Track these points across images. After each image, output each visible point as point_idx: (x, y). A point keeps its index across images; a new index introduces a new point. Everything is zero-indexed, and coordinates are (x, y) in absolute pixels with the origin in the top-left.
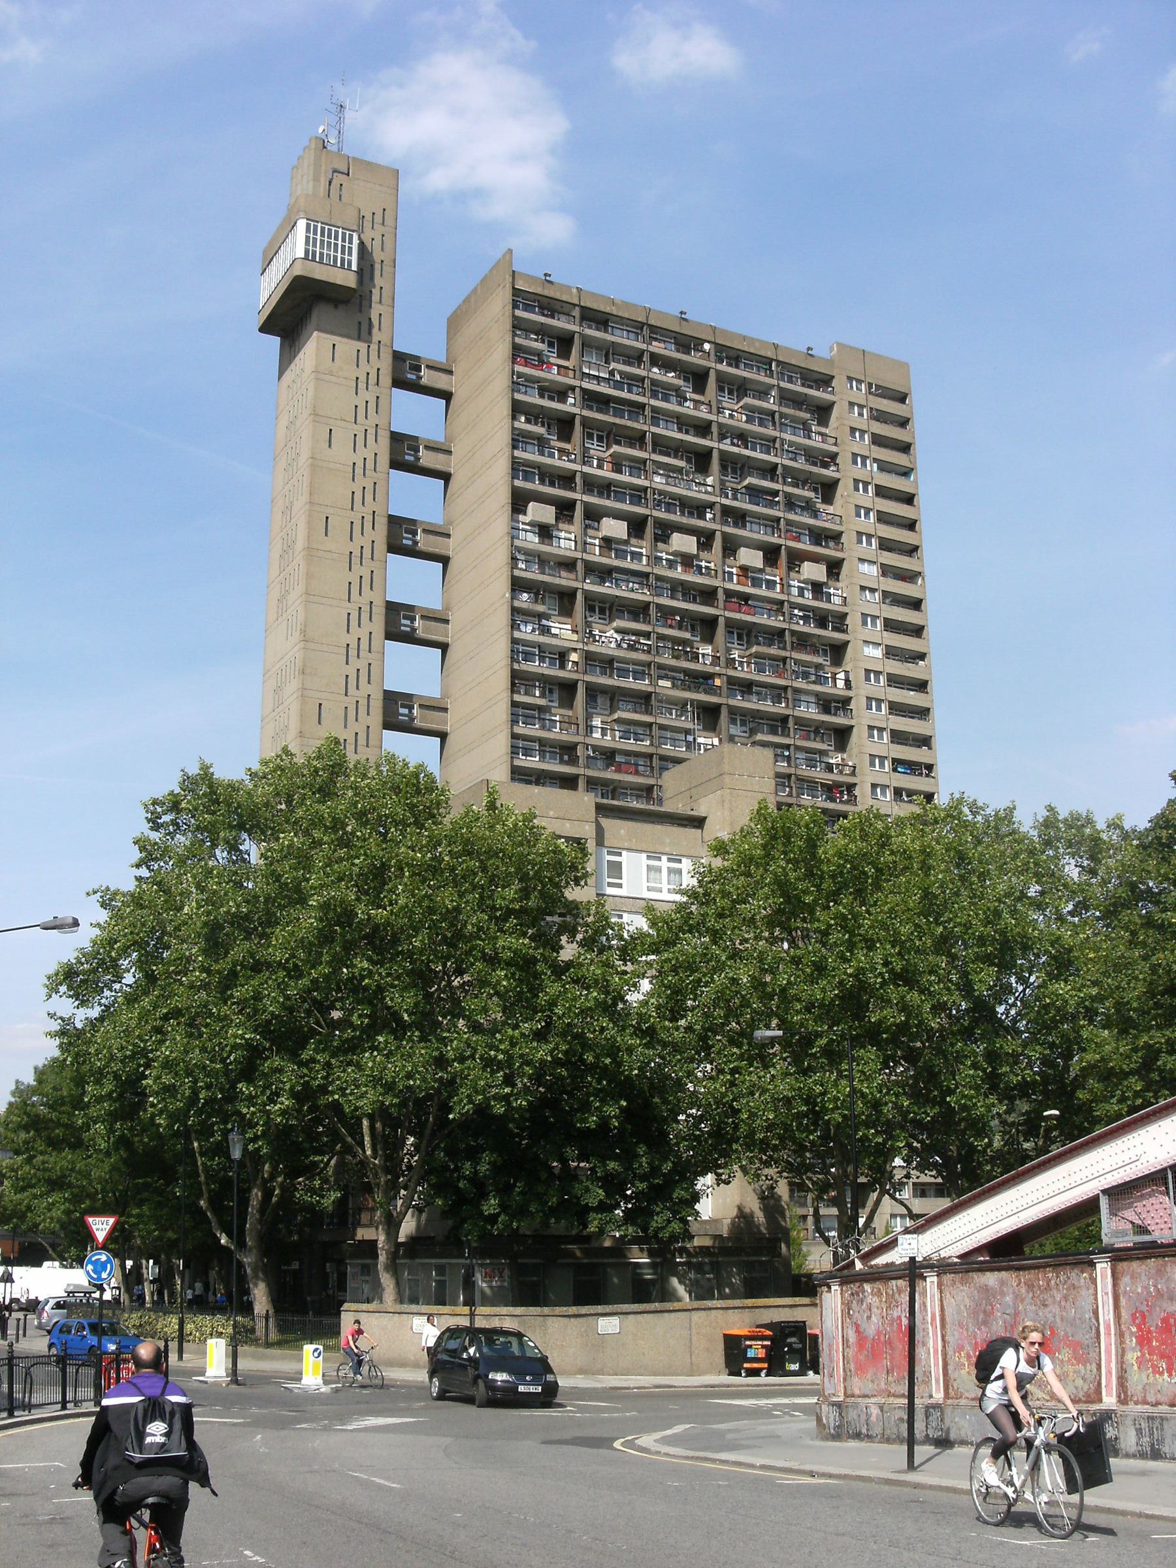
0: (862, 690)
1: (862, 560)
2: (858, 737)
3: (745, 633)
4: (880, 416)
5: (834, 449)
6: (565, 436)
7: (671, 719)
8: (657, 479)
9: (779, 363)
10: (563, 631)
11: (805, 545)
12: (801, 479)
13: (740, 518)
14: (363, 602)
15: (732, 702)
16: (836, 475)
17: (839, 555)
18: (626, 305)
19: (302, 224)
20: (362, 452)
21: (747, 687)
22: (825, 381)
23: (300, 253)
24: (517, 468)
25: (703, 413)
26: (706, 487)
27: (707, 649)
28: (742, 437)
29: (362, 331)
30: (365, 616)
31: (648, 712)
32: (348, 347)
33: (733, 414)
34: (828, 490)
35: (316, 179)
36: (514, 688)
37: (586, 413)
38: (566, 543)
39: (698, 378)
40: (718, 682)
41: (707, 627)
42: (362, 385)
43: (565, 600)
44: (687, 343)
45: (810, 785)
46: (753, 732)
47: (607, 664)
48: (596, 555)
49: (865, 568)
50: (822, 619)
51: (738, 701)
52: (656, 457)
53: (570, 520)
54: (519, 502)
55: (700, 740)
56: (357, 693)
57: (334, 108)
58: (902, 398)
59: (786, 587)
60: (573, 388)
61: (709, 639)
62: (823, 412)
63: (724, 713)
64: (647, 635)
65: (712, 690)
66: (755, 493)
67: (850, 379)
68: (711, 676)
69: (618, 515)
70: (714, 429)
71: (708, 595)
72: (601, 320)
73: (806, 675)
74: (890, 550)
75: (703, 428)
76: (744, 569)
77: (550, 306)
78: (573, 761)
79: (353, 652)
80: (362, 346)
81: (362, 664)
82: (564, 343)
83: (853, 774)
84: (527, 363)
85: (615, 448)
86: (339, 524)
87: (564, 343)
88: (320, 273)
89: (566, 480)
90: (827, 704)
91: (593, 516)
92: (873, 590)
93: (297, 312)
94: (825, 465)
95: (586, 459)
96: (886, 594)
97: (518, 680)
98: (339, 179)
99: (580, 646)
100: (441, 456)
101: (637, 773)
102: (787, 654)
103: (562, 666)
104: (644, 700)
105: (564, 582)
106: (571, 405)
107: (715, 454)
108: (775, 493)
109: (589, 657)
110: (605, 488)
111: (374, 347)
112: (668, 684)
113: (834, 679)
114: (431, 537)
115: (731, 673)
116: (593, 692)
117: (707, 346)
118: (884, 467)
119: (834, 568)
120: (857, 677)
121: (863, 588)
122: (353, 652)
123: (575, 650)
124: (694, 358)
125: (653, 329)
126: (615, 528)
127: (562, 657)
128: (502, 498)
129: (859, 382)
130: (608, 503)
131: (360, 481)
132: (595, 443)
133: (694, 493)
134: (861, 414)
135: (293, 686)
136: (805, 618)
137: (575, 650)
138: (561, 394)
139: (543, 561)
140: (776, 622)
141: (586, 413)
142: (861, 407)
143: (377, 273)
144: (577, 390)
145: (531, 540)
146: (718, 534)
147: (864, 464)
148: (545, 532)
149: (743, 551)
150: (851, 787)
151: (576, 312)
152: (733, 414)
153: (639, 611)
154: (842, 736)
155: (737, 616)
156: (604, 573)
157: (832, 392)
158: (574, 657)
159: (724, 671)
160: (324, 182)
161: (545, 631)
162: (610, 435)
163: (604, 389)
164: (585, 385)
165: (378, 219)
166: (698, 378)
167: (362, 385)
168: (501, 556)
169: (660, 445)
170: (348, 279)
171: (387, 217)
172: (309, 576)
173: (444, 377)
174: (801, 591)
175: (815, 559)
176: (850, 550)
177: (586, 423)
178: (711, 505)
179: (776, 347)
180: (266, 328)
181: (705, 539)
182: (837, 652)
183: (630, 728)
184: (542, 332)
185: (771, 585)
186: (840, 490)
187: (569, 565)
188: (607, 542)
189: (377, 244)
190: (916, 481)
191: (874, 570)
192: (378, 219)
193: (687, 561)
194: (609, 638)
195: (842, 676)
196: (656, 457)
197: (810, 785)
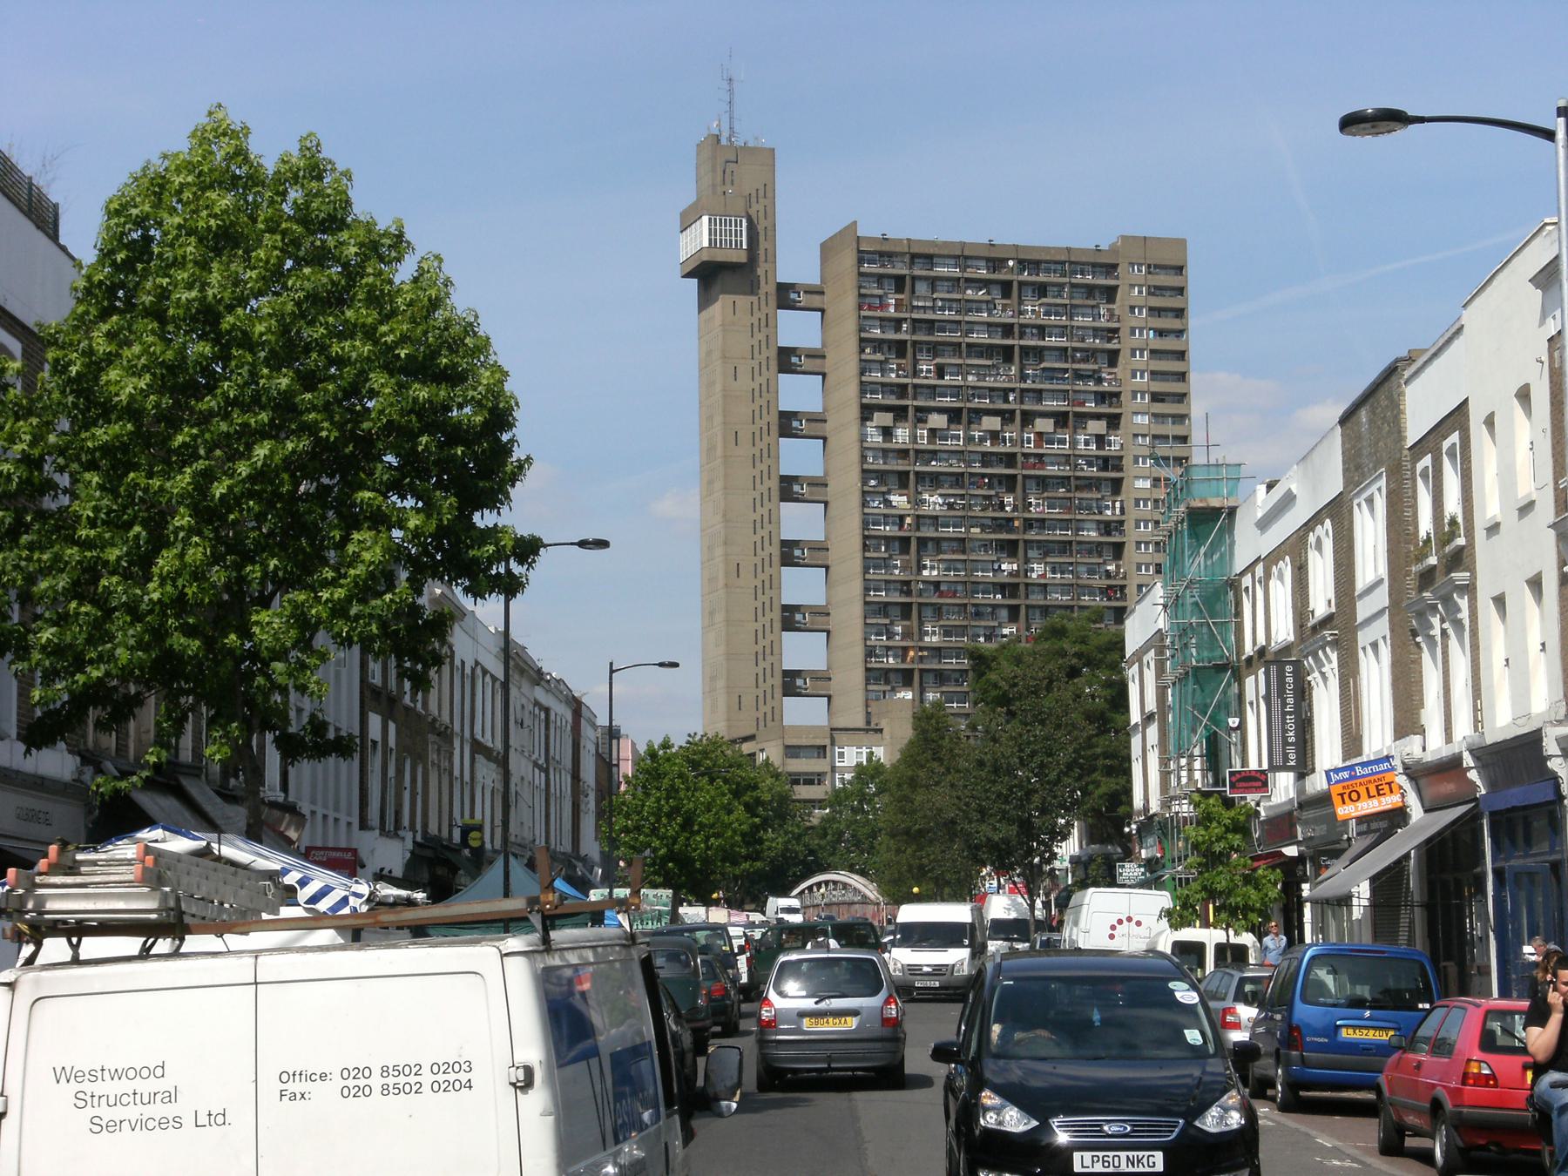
0: (1132, 515)
1: (1137, 413)
2: (1129, 551)
3: (1043, 483)
4: (1156, 290)
5: (1115, 325)
6: (901, 353)
7: (982, 556)
8: (970, 378)
9: (1071, 263)
10: (899, 500)
11: (1091, 406)
12: (1090, 354)
13: (1039, 395)
15: (1027, 537)
16: (1117, 347)
17: (1117, 411)
18: (946, 244)
19: (705, 219)
20: (759, 380)
21: (1042, 523)
22: (1111, 269)
23: (706, 244)
24: (864, 388)
25: (1007, 318)
26: (1006, 376)
27: (1009, 499)
28: (1042, 331)
29: (753, 288)
30: (766, 498)
31: (964, 552)
32: (743, 301)
33: (1032, 310)
34: (1113, 357)
35: (714, 170)
36: (865, 548)
37: (915, 338)
39: (1006, 288)
40: (1016, 523)
41: (1010, 483)
42: (756, 329)
43: (902, 479)
44: (996, 263)
45: (1090, 590)
46: (1046, 554)
47: (935, 520)
48: (924, 443)
49: (1139, 419)
50: (1105, 463)
51: (1032, 535)
52: (969, 362)
53: (905, 418)
54: (867, 412)
55: (1004, 567)
57: (725, 85)
58: (1179, 269)
59: (1074, 443)
61: (1011, 490)
62: (1110, 293)
63: (1021, 545)
64: (962, 497)
65: (1011, 530)
66: (1050, 374)
67: (1132, 265)
68: (1011, 520)
69: (940, 410)
70: (1016, 330)
71: (1010, 460)
72: (929, 259)
73: (1089, 508)
74: (1162, 401)
75: (1007, 330)
76: (1040, 435)
77: (886, 256)
78: (909, 593)
79: (758, 525)
80: (754, 299)
81: (765, 533)
82: (899, 283)
83: (1125, 578)
84: (870, 308)
85: (938, 360)
86: (745, 437)
87: (899, 283)
88: (720, 257)
89: (901, 390)
90: (1107, 527)
91: (922, 414)
92: (1144, 436)
93: (710, 275)
94: (1109, 340)
95: (916, 373)
97: (868, 542)
98: (731, 166)
100: (818, 361)
101: (954, 596)
103: (901, 526)
104: (962, 544)
105: (900, 468)
106: (904, 335)
107: (1017, 350)
108: (1066, 371)
110: (933, 391)
111: (763, 298)
112: (978, 530)
113: (1114, 508)
114: (813, 425)
115: (1027, 515)
116: (922, 542)
117: (1011, 263)
118: (1161, 333)
119: (1114, 421)
120: (1129, 505)
121: (1136, 436)
122: (758, 525)
124: (1002, 276)
125: (967, 258)
126: (938, 421)
127: (902, 518)
128: (854, 412)
129: (1140, 265)
130: (932, 404)
131: (758, 402)
133: (1001, 382)
134: (1140, 292)
135: (719, 551)
136: (1090, 464)
138: (897, 324)
139: (885, 452)
140: (1066, 471)
142: (1140, 286)
143: (761, 238)
145: (876, 438)
147: (1141, 334)
148: (887, 432)
149: (1038, 421)
150: (1123, 588)
151: (907, 258)
152: (1032, 310)
153: (958, 479)
154: (1118, 549)
155: (1032, 472)
156: (934, 454)
157: (1117, 278)
158: (908, 520)
160: (719, 173)
161: (888, 503)
162: (935, 349)
163: (929, 316)
164: (915, 316)
165: (761, 193)
166: (1006, 288)
167: (756, 329)
168: (854, 455)
170: (742, 258)
171: (767, 191)
172: (726, 476)
173: (817, 297)
174: (1087, 443)
175: (1098, 417)
176: (1127, 405)
177: (915, 343)
178: (1013, 390)
179: (1069, 250)
180: (688, 275)
181: (1007, 416)
182: (1116, 486)
183: (950, 565)
184: (880, 278)
185: (1062, 442)
186: (1121, 360)
187: (903, 453)
188: (933, 432)
189: (761, 214)
190: (1187, 341)
191: (1146, 420)
192: (761, 193)
193: (995, 436)
194: (934, 501)
195: (1118, 505)
196: (969, 362)
197: (1090, 590)
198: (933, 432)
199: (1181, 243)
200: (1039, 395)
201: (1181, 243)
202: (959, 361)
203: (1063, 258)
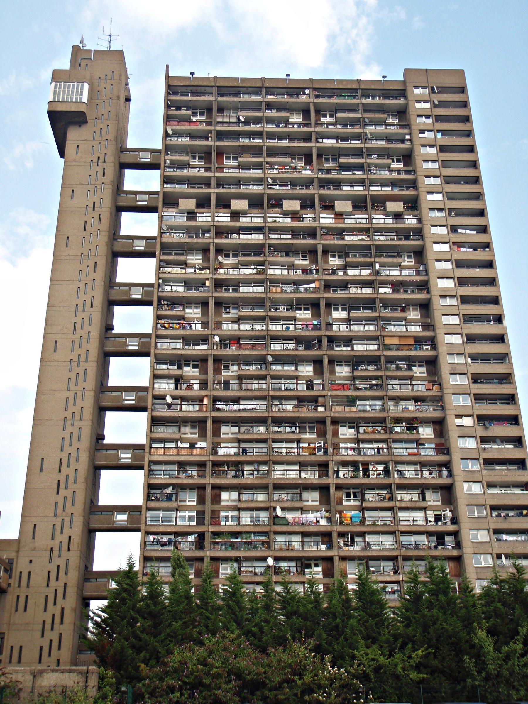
13: (338, 184)
14: (89, 280)
38: (203, 219)
56: (82, 332)
60: (210, 132)
71: (312, 233)
96: (450, 210)
99: (211, 276)
102: (372, 260)
109: (219, 284)
123: (208, 279)
132: (232, 161)
137: (208, 279)
141: (218, 143)
144: (213, 132)
146: (316, 196)
151: (214, 90)
159: (321, 277)
164: (220, 128)
169: (272, 152)
198: (235, 215)
199: (461, 73)
200: (338, 184)
201: (461, 73)
202: (261, 159)
203: (354, 86)
